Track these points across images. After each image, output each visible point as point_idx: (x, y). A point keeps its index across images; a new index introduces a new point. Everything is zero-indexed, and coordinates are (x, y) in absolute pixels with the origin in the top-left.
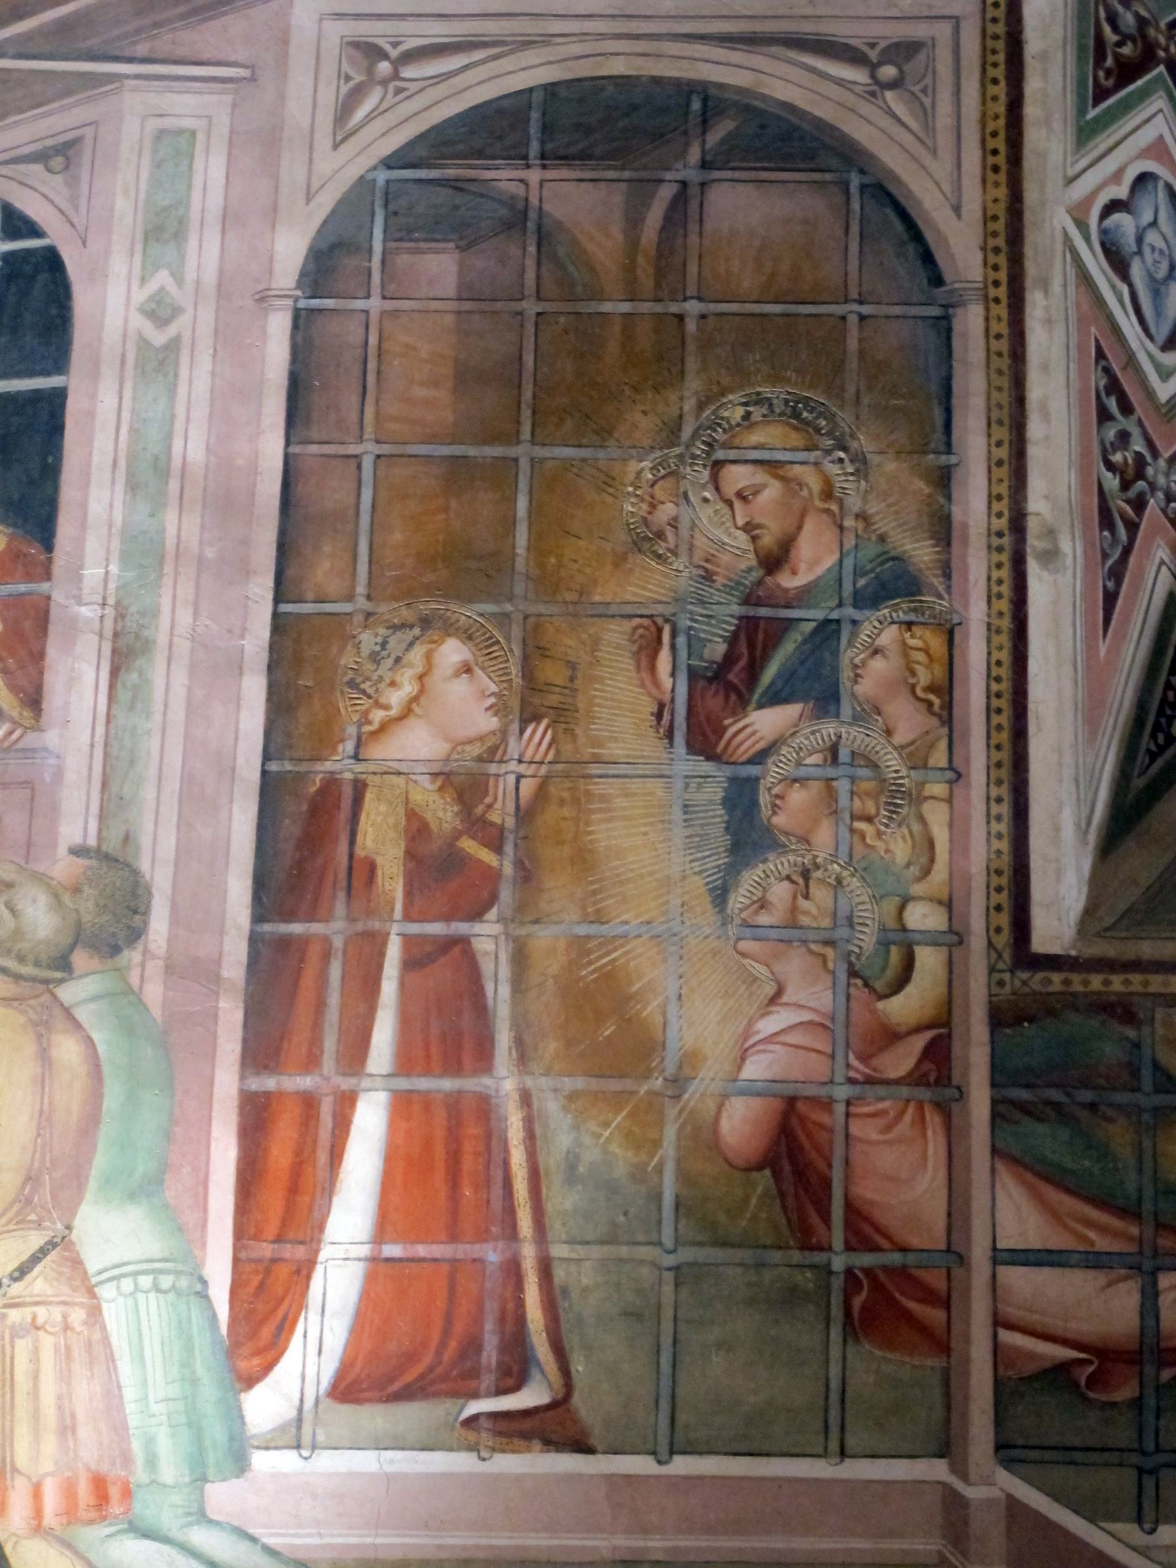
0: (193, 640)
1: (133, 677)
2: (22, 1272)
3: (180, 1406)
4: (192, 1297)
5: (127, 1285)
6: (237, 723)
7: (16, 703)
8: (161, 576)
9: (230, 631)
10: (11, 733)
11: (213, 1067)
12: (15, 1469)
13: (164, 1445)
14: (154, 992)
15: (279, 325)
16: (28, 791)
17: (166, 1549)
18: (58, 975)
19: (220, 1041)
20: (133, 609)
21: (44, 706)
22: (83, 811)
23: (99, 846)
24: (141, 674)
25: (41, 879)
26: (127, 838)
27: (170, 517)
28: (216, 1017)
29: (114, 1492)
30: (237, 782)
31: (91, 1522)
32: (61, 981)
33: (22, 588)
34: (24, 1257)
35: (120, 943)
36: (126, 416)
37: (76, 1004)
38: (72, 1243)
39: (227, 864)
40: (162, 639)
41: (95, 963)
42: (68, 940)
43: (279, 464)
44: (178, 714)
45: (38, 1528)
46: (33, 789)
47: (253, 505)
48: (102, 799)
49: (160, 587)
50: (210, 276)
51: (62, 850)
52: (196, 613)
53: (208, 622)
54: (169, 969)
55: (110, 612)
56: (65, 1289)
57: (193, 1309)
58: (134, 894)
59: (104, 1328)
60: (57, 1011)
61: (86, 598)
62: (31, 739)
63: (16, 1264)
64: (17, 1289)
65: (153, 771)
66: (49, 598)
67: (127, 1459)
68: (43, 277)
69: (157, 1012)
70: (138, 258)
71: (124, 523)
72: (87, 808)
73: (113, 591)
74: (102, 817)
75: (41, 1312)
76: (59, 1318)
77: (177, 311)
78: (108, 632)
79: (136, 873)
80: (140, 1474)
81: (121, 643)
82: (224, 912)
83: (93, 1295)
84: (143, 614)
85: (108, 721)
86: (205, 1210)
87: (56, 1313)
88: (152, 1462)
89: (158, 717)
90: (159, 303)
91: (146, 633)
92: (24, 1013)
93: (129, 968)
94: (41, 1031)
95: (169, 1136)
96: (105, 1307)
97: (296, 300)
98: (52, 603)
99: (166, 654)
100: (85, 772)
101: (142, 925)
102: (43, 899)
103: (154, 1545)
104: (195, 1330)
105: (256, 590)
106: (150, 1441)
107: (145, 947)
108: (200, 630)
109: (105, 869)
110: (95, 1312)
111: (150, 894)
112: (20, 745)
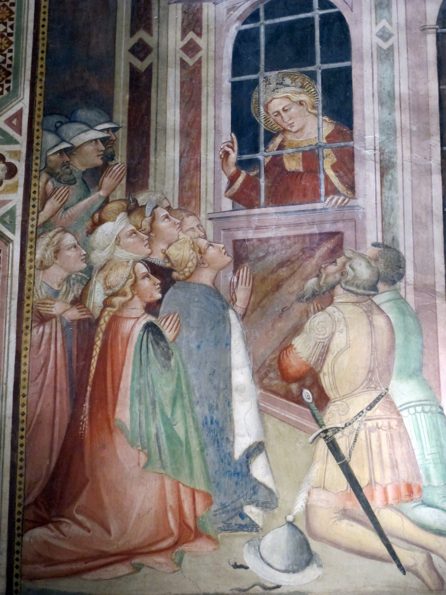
0: (411, 162)
1: (390, 177)
2: (371, 407)
3: (437, 456)
4: (438, 414)
5: (412, 410)
6: (432, 193)
7: (345, 189)
8: (396, 138)
9: (425, 158)
10: (344, 200)
11: (437, 325)
12: (376, 483)
13: (432, 471)
14: (411, 298)
15: (431, 39)
16: (354, 223)
17: (437, 510)
18: (373, 293)
19: (438, 316)
20: (387, 151)
21: (356, 189)
22: (376, 229)
23: (383, 242)
24: (392, 176)
25: (362, 256)
26: (393, 239)
27: (397, 115)
28: (436, 307)
29: (415, 490)
30: (434, 216)
31: (407, 502)
32: (374, 295)
33: (343, 144)
34: (371, 401)
35: (395, 279)
36: (376, 76)
37: (381, 304)
38: (389, 395)
39: (434, 248)
40: (399, 162)
41: (387, 288)
42: (375, 279)
43: (437, 93)
44: (408, 191)
45: (387, 505)
46: (355, 221)
47: (429, 109)
48: (382, 224)
49: (396, 142)
50: (402, 22)
51: (369, 245)
52: (411, 152)
53: (416, 155)
54: (415, 289)
55: (378, 152)
56: (388, 413)
57: (438, 419)
58: (399, 261)
59: (405, 427)
60: (374, 306)
61: (367, 147)
62: (352, 202)
63: (368, 404)
64: (369, 413)
65: (400, 213)
66: (353, 148)
67: (419, 477)
68: (337, 24)
69: (413, 305)
70: (373, 15)
71: (379, 118)
72: (377, 228)
73: (378, 144)
74: (383, 231)
75: (380, 422)
76: (387, 424)
77: (391, 35)
78: (378, 160)
79: (398, 252)
80: (424, 483)
81: (383, 164)
82: (434, 267)
83: (399, 415)
84: (391, 152)
85: (381, 195)
86: (439, 381)
87: (386, 422)
88: (428, 478)
89: (400, 192)
90: (383, 32)
91: (393, 160)
92: (362, 308)
93: (400, 289)
94: (369, 313)
95: (422, 353)
96: (405, 420)
97: (437, 29)
98: (355, 150)
99: (401, 167)
100: (374, 214)
101: (403, 273)
102: (364, 263)
103: (432, 509)
104: (440, 428)
105: (434, 142)
106: (427, 470)
107: (405, 281)
108: (414, 158)
109: (386, 251)
110: (400, 421)
111: (405, 260)
112: (348, 204)
